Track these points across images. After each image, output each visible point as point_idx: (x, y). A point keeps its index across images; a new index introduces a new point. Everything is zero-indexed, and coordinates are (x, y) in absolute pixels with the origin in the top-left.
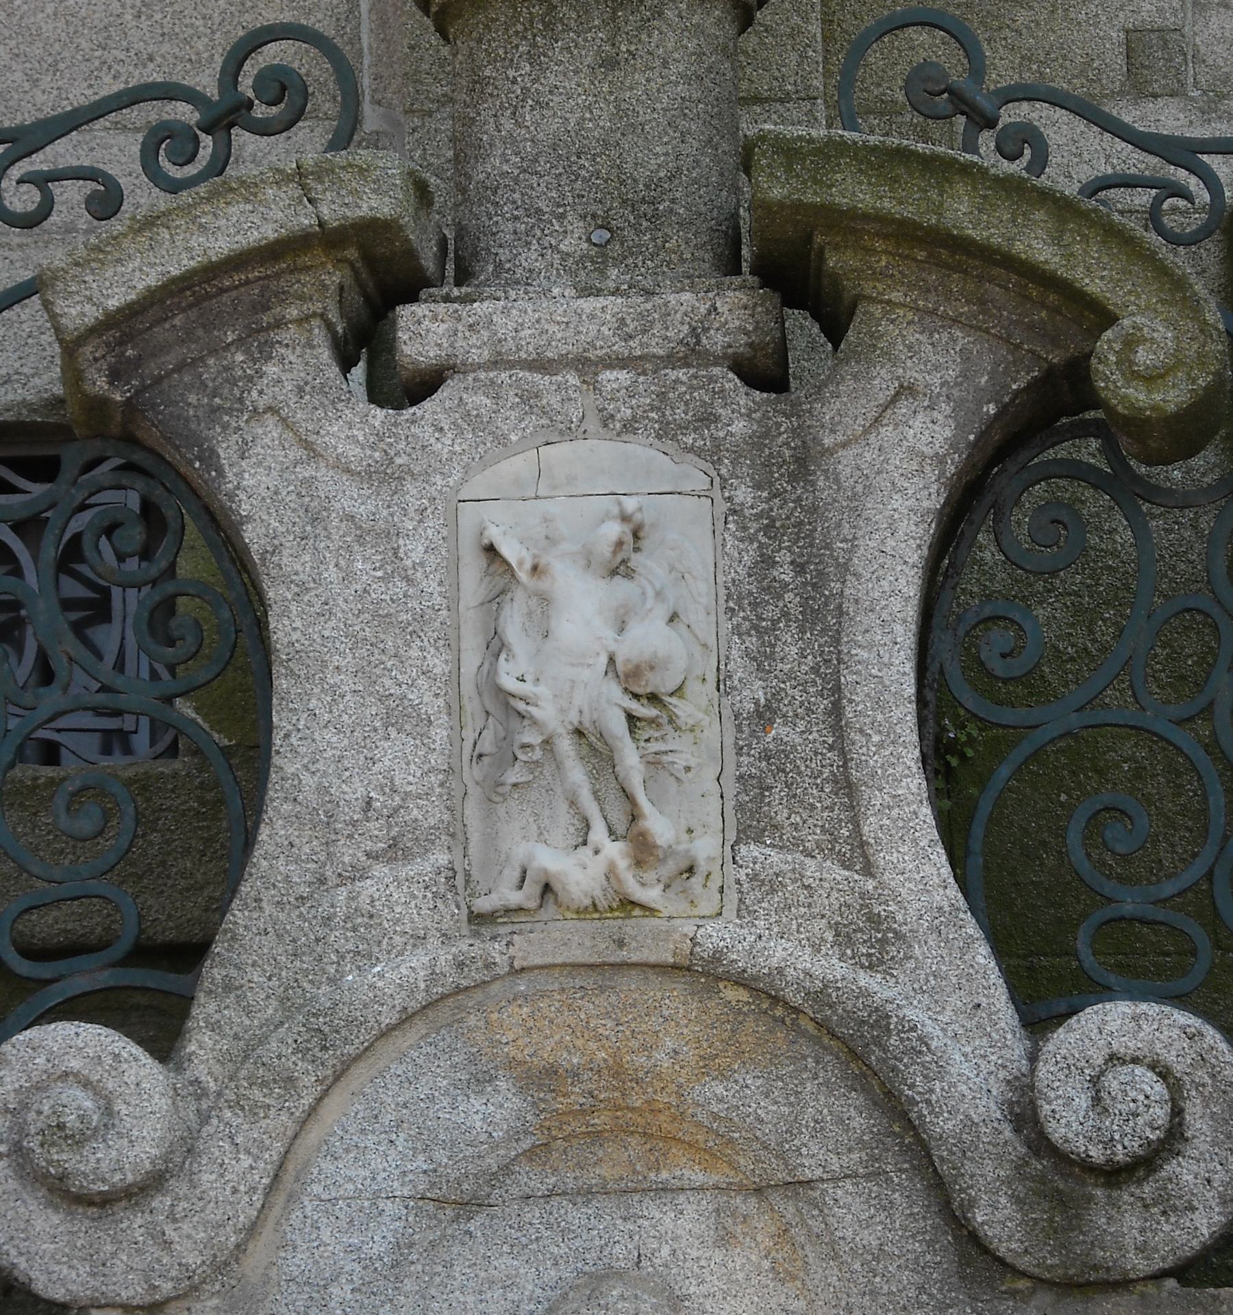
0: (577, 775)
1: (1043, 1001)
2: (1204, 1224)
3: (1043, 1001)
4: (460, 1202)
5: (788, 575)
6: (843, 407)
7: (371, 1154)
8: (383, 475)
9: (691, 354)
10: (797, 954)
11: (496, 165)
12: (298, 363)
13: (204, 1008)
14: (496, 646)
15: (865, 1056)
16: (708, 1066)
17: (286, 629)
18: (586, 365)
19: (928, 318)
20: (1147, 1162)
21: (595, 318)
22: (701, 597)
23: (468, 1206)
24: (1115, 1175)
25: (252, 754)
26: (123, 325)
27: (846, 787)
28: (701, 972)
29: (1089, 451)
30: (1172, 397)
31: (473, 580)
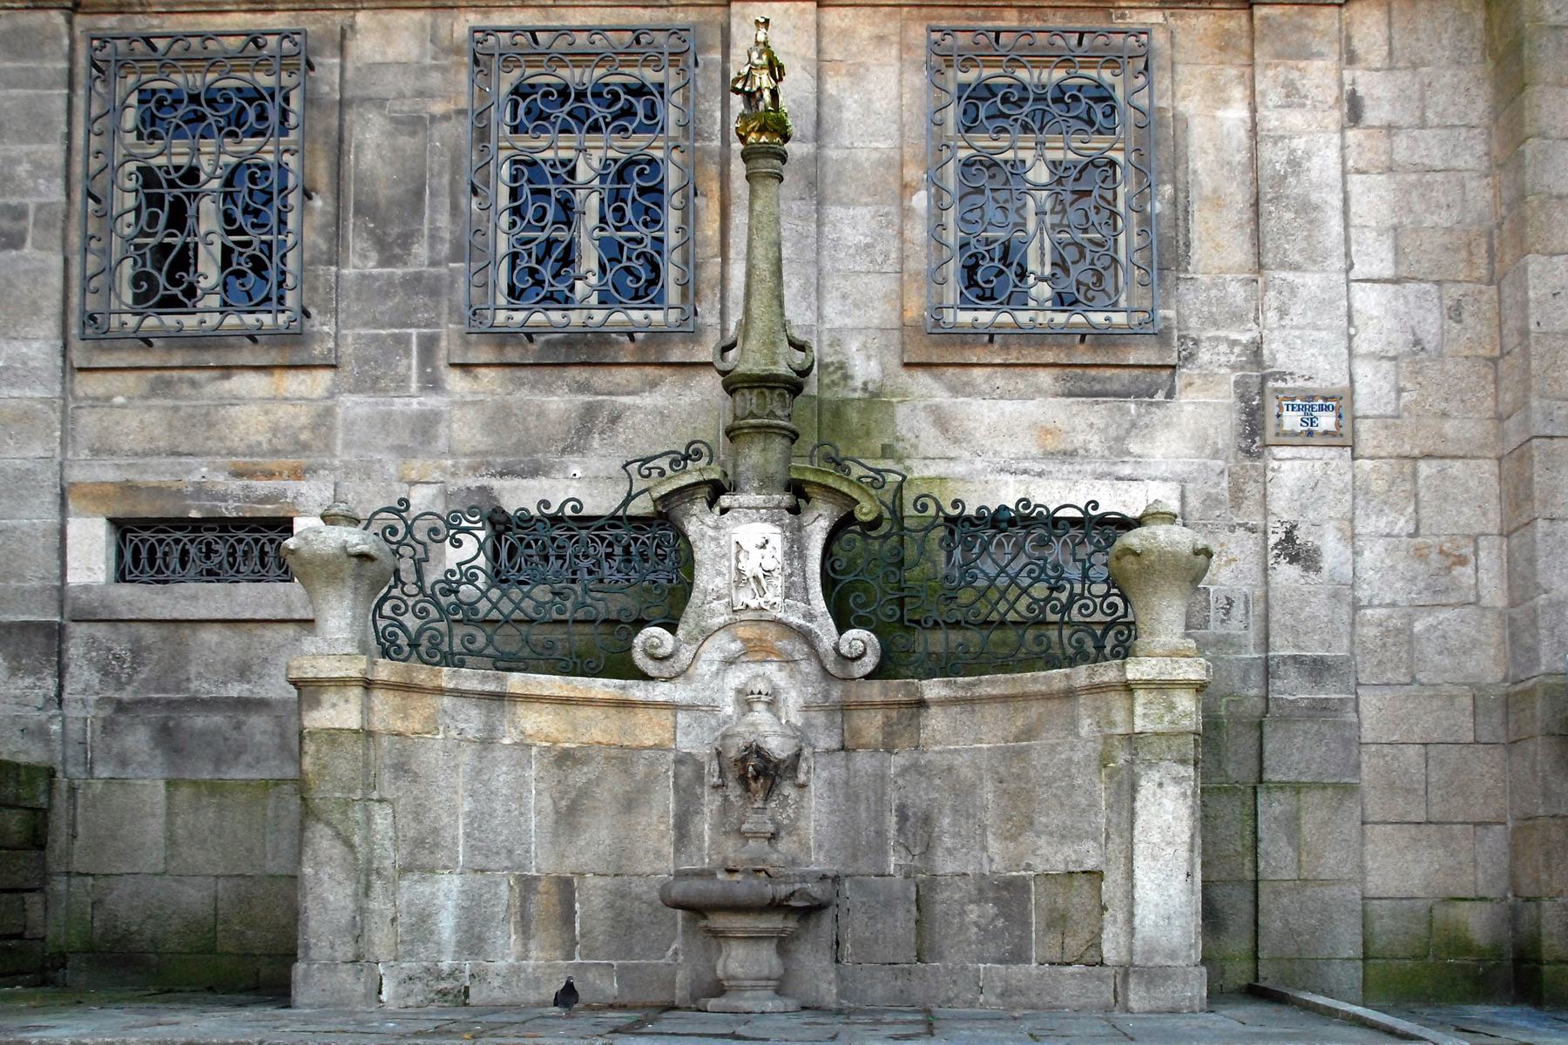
0: (753, 585)
1: (842, 628)
2: (870, 668)
3: (842, 628)
4: (729, 662)
5: (796, 549)
6: (807, 518)
7: (713, 652)
8: (717, 528)
9: (778, 507)
10: (795, 619)
11: (741, 469)
12: (700, 506)
13: (681, 625)
14: (738, 561)
15: (806, 636)
16: (778, 639)
17: (698, 556)
18: (757, 508)
19: (825, 501)
20: (859, 657)
21: (759, 499)
22: (779, 555)
23: (731, 663)
24: (854, 659)
25: (691, 585)
26: (664, 498)
27: (806, 589)
28: (777, 622)
29: (858, 528)
30: (870, 518)
31: (734, 548)
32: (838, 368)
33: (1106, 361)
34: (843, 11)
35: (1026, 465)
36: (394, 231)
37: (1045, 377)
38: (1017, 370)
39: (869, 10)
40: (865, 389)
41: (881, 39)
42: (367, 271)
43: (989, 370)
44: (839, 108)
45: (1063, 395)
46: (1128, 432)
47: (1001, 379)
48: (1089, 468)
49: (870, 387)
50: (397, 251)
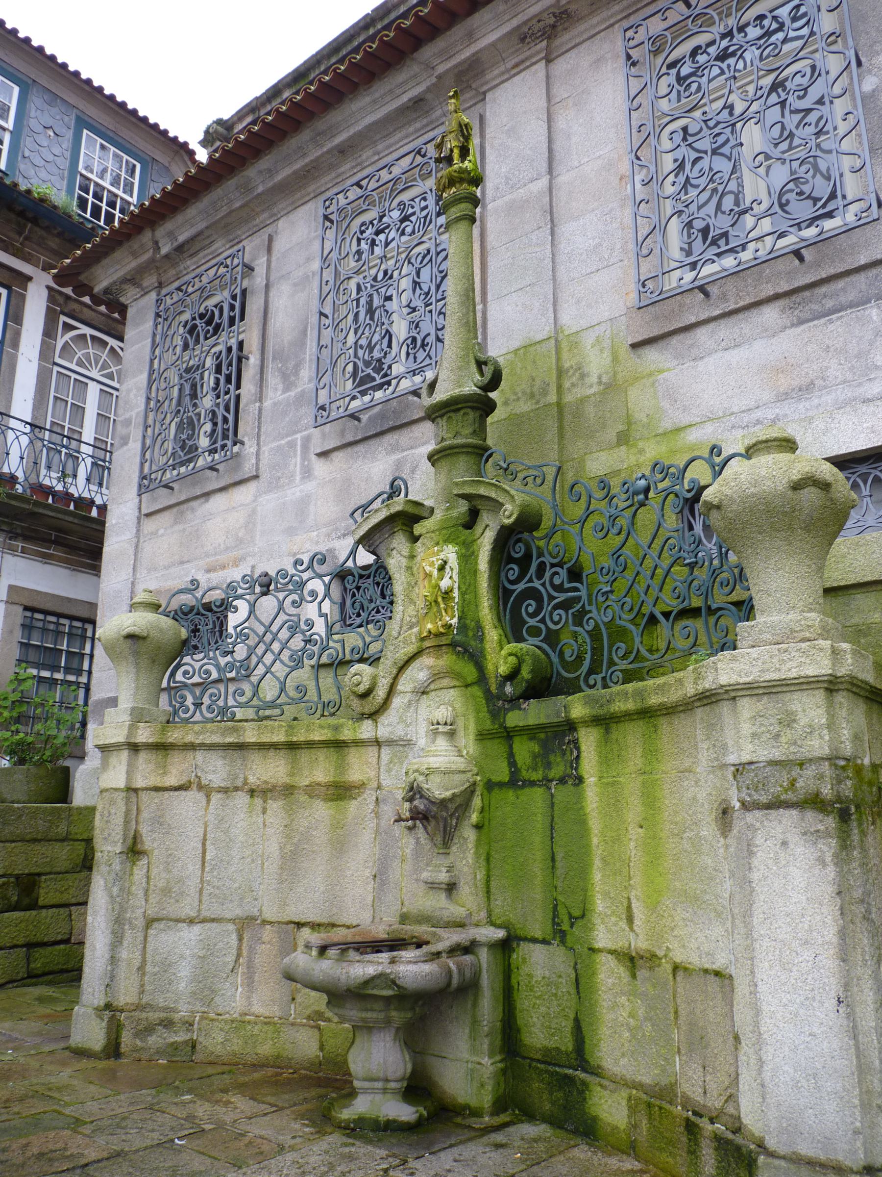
32: (576, 371)
33: (832, 271)
34: (568, 55)
35: (758, 414)
36: (291, 365)
37: (770, 314)
38: (741, 316)
39: (588, 43)
40: (600, 383)
41: (599, 61)
42: (276, 400)
43: (712, 325)
44: (569, 137)
45: (793, 325)
46: (871, 343)
47: (725, 330)
48: (829, 399)
49: (604, 380)
50: (293, 378)
